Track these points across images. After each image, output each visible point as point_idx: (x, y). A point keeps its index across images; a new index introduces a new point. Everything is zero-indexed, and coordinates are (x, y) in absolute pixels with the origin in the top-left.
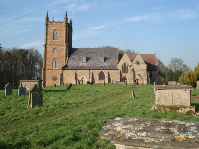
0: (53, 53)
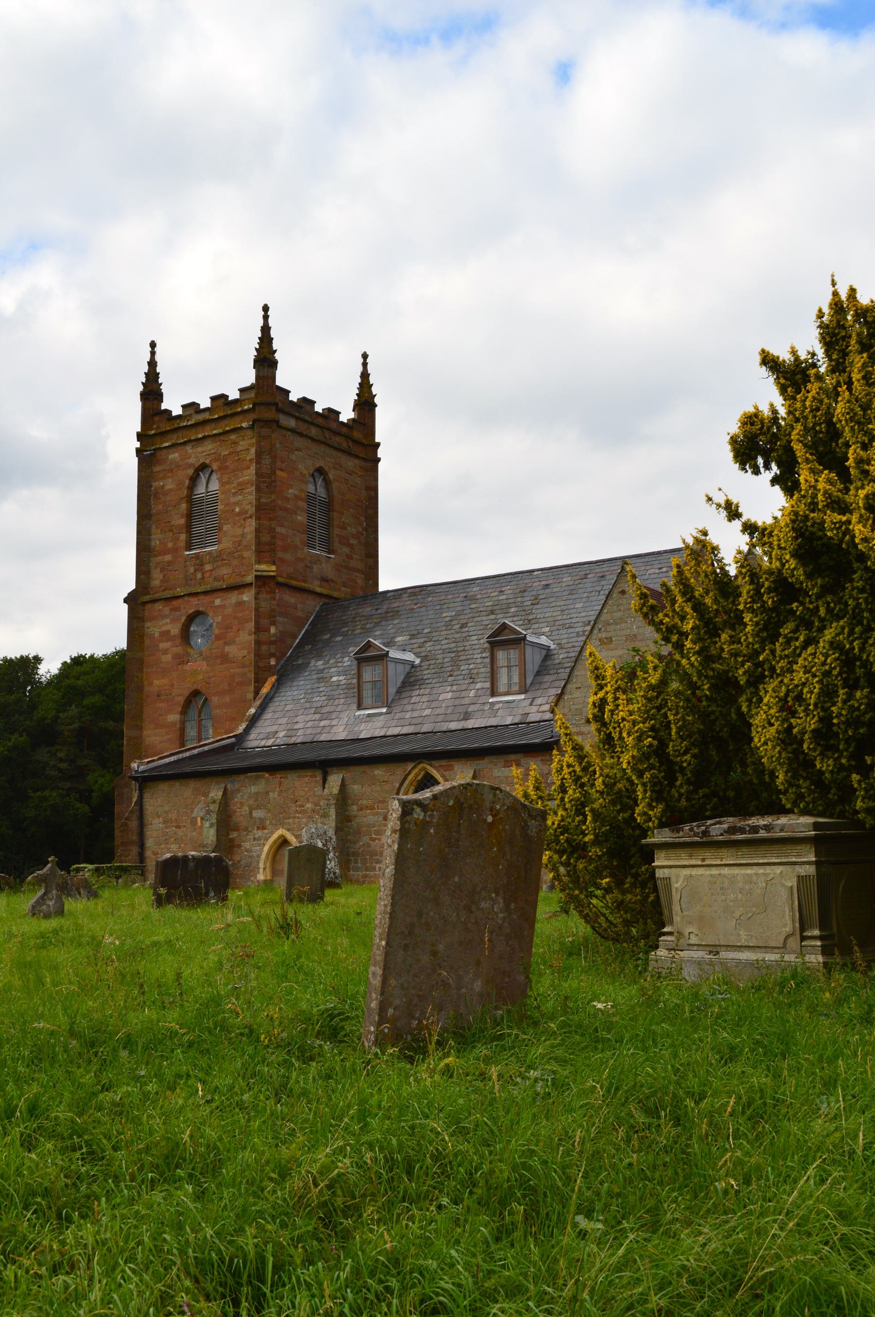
0: (179, 650)
